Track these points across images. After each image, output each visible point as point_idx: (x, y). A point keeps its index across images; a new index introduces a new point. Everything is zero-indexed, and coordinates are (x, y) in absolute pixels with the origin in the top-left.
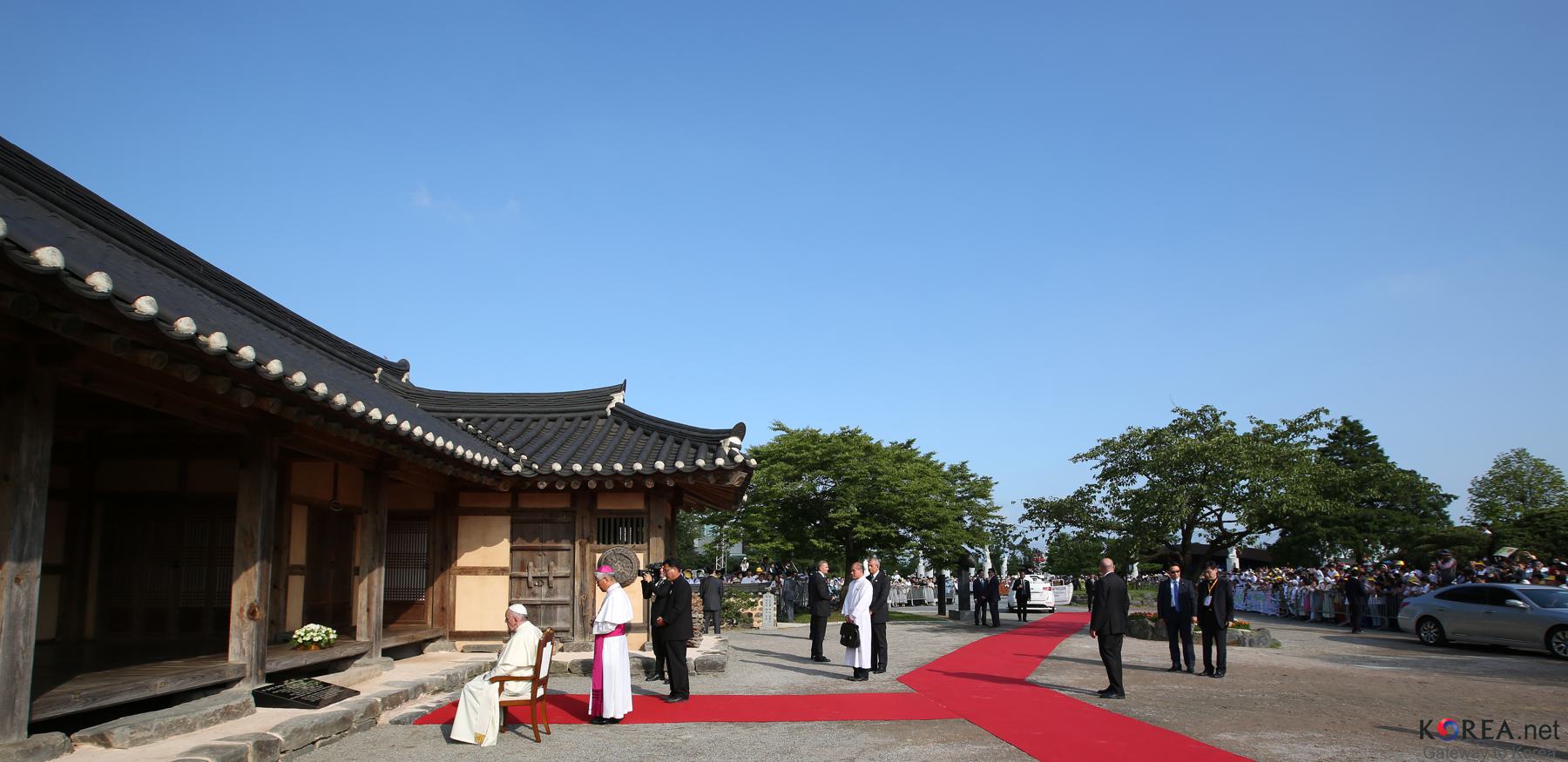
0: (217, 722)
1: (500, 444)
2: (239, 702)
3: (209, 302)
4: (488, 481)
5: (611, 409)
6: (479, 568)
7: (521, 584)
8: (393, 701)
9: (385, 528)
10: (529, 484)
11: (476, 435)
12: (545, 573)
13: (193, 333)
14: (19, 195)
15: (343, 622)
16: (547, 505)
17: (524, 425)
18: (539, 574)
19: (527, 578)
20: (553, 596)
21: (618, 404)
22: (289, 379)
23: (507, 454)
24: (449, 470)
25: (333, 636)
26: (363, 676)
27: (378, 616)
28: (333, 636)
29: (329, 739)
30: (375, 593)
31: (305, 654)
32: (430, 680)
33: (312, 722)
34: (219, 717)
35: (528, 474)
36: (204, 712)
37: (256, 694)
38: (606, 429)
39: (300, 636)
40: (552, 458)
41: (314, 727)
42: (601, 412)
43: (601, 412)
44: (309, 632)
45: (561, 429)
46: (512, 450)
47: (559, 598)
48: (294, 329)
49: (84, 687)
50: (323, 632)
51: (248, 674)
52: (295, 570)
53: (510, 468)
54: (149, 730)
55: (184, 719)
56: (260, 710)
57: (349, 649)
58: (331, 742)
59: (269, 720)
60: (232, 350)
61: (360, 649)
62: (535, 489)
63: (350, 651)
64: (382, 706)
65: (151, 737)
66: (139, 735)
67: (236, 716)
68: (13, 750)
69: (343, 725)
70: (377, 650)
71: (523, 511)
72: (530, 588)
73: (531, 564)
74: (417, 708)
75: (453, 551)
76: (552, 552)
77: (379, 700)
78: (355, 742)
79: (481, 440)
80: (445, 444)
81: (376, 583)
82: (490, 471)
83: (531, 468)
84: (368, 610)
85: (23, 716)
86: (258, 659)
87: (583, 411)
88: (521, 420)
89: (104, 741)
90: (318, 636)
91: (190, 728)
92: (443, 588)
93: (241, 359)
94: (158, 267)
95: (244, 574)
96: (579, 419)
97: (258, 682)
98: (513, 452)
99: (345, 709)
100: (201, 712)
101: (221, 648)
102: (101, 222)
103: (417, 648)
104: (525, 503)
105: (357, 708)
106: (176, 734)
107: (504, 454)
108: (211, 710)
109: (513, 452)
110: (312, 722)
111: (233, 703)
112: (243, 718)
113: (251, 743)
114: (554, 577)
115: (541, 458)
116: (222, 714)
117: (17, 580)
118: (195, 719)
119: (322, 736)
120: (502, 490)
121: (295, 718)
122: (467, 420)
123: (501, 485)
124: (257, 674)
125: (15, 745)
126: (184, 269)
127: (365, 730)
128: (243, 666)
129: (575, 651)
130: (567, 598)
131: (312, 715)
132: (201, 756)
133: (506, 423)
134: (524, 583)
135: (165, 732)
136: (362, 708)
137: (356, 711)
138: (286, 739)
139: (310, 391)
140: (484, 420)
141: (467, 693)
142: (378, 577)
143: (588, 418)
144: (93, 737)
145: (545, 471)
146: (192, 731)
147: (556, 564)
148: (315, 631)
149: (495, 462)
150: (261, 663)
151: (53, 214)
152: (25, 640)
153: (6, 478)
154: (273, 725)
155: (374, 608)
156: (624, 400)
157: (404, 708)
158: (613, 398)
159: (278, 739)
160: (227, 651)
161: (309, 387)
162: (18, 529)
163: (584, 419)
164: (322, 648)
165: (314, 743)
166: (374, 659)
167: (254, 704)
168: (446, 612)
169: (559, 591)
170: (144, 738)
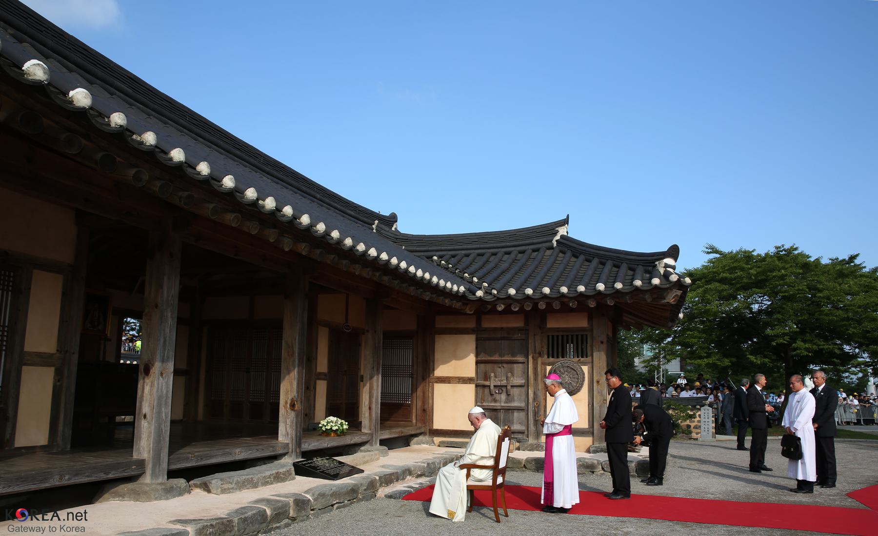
0: (272, 484)
1: (466, 275)
2: (284, 470)
3: (266, 180)
4: (457, 305)
5: (557, 241)
6: (451, 377)
7: (484, 391)
8: (388, 479)
9: (381, 345)
10: (489, 307)
11: (447, 269)
12: (504, 382)
13: (255, 199)
14: (166, 124)
15: (351, 414)
16: (505, 325)
17: (484, 258)
18: (499, 383)
19: (489, 386)
21: (562, 236)
22: (315, 228)
23: (472, 282)
24: (427, 296)
25: (345, 427)
26: (367, 458)
27: (376, 413)
28: (345, 427)
30: (375, 395)
31: (327, 439)
32: (414, 466)
33: (331, 489)
34: (272, 480)
35: (489, 298)
36: (264, 475)
37: (295, 465)
38: (553, 258)
39: (323, 425)
40: (508, 284)
41: (333, 492)
42: (548, 244)
43: (548, 244)
44: (329, 423)
45: (515, 260)
46: (475, 279)
47: (516, 404)
48: (318, 196)
49: (196, 450)
50: (339, 423)
51: (290, 450)
52: (320, 376)
53: (474, 294)
54: (231, 483)
55: (252, 478)
56: (298, 478)
57: (356, 438)
58: (344, 506)
59: (303, 485)
60: (278, 209)
61: (364, 438)
62: (494, 311)
63: (357, 439)
65: (233, 488)
66: (226, 486)
67: (283, 480)
68: (159, 487)
69: (353, 493)
70: (376, 439)
71: (486, 330)
72: (492, 395)
73: (492, 375)
74: (404, 487)
75: (432, 364)
76: (509, 366)
77: (377, 478)
78: (360, 508)
79: (451, 272)
80: (424, 275)
81: (375, 387)
82: (458, 296)
83: (491, 294)
84: (370, 408)
85: (165, 466)
86: (296, 440)
87: (533, 244)
88: (482, 255)
89: (206, 488)
90: (335, 426)
91: (255, 486)
92: (424, 393)
93: (284, 215)
94: (237, 161)
95: (287, 377)
96: (530, 251)
97: (297, 458)
98: (476, 281)
99: (353, 482)
100: (262, 475)
101: (273, 432)
102: (207, 135)
103: (404, 441)
104: (486, 324)
105: (362, 482)
106: (247, 489)
107: (469, 282)
108: (268, 473)
109: (476, 281)
110: (331, 489)
111: (281, 470)
112: (287, 482)
114: (511, 386)
115: (498, 285)
116: (275, 478)
117: (162, 374)
118: (258, 479)
119: (338, 501)
120: (468, 312)
121: (320, 485)
122: (440, 257)
123: (468, 308)
125: (161, 484)
126: (252, 160)
128: (287, 444)
129: (530, 450)
130: (523, 405)
132: (262, 505)
133: (470, 258)
134: (487, 390)
135: (241, 486)
136: (365, 483)
137: (361, 484)
138: (315, 500)
139: (328, 237)
140: (454, 256)
141: (442, 477)
142: (377, 383)
143: (537, 250)
144: (200, 484)
145: (502, 296)
146: (256, 487)
147: (513, 375)
148: (333, 422)
149: (462, 289)
150: (299, 444)
151: (183, 134)
152: (166, 416)
153: (157, 306)
155: (374, 406)
156: (567, 232)
158: (558, 231)
159: (309, 499)
160: (277, 434)
161: (327, 234)
162: (162, 340)
163: (534, 251)
164: (338, 436)
165: (332, 505)
166: (374, 447)
168: (427, 413)
169: (516, 398)
170: (229, 489)
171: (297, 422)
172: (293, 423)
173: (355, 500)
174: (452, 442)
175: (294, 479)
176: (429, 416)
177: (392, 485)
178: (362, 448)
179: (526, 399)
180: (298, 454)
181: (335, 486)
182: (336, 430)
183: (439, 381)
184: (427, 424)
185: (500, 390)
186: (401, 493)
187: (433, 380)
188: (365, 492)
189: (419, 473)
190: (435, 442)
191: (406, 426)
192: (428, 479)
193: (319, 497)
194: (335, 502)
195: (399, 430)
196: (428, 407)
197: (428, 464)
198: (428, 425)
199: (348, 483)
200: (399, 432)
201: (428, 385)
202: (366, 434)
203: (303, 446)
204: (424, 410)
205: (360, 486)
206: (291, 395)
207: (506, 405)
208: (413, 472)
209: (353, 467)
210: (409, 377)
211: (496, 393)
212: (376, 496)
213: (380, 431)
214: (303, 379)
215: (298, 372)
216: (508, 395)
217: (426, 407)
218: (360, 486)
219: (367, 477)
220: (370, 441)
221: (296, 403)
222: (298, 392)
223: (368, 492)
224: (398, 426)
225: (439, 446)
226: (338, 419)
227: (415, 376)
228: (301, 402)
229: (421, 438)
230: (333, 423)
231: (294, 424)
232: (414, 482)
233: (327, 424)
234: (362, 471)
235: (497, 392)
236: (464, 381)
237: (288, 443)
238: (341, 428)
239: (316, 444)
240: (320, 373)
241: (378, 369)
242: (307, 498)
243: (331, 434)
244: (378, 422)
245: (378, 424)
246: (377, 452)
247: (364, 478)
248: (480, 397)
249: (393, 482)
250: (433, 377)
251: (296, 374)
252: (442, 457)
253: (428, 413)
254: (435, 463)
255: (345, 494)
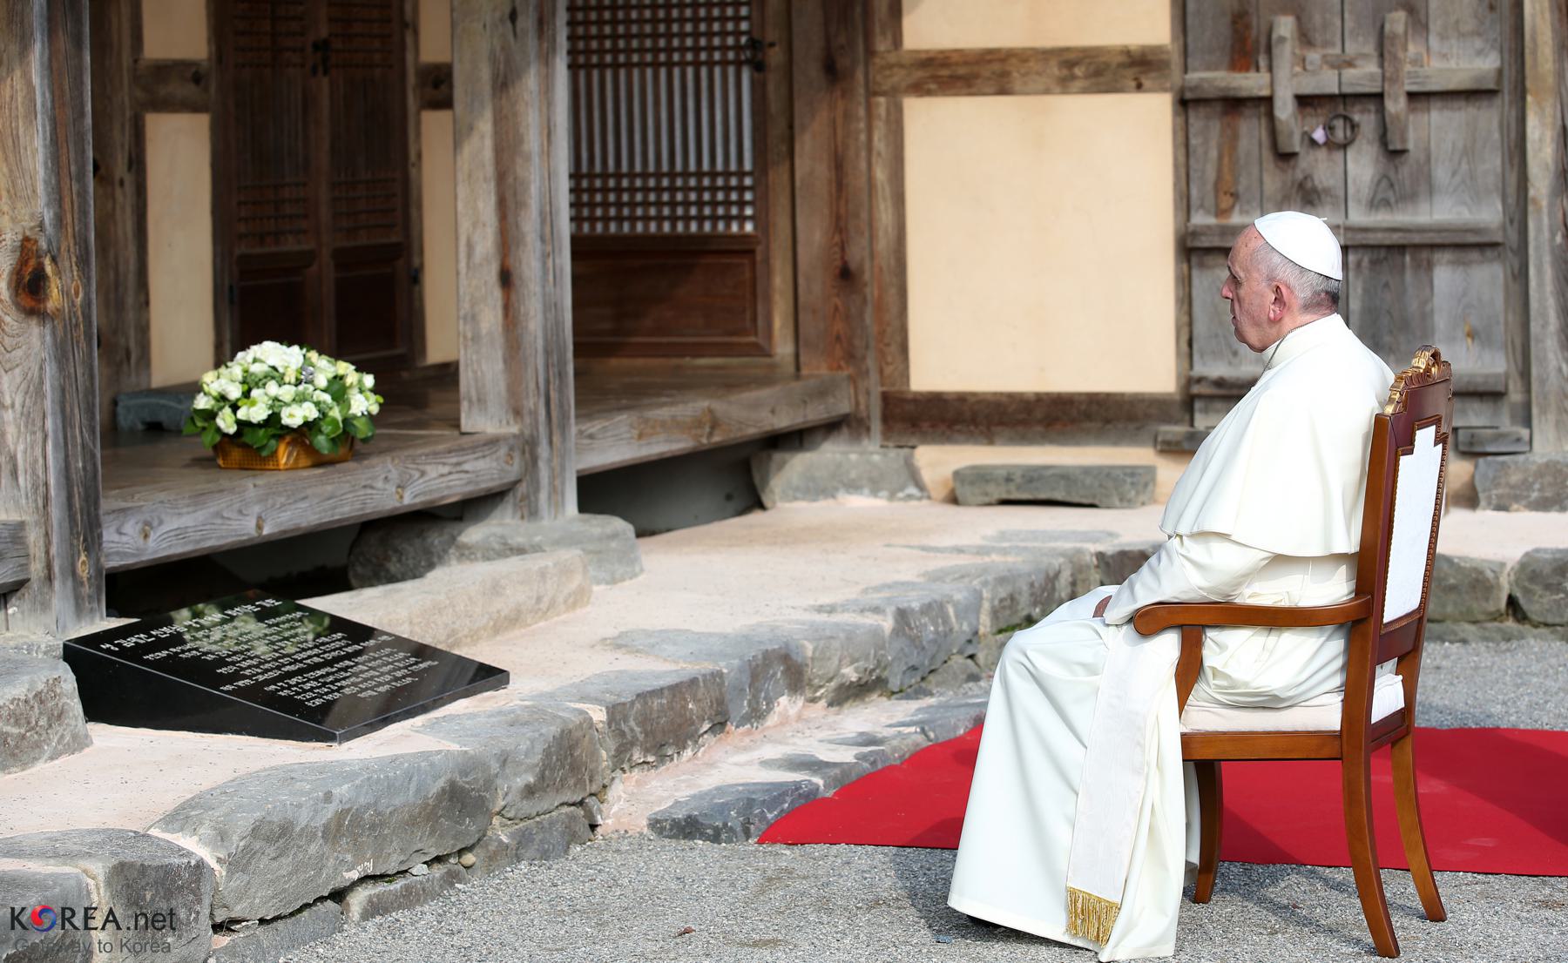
7: (1235, 137)
12: (1363, 75)
18: (1327, 82)
19: (1268, 101)
20: (1409, 197)
26: (517, 596)
27: (550, 306)
28: (363, 403)
29: (398, 885)
30: (534, 190)
31: (252, 486)
32: (816, 632)
33: (328, 797)
37: (77, 655)
39: (222, 398)
41: (340, 816)
44: (260, 382)
50: (322, 381)
51: (36, 569)
56: (107, 736)
57: (433, 471)
58: (410, 899)
61: (483, 471)
64: (612, 744)
72: (1285, 157)
73: (1285, 26)
74: (766, 764)
77: (599, 715)
81: (533, 141)
84: (506, 278)
90: (300, 399)
92: (839, 165)
99: (455, 747)
105: (508, 743)
110: (328, 797)
112: (42, 768)
113: (98, 869)
114: (1412, 96)
119: (369, 868)
124: (74, 573)
127: (545, 855)
129: (1543, 505)
130: (1489, 215)
131: (321, 769)
134: (1251, 131)
136: (529, 746)
137: (504, 760)
138: (235, 864)
154: (170, 802)
155: (530, 265)
157: (711, 765)
159: (200, 866)
164: (320, 462)
165: (339, 895)
166: (546, 522)
167: (76, 706)
169: (1441, 173)
171: (63, 390)
172: (39, 393)
173: (469, 858)
174: (1033, 475)
175: (79, 743)
176: (880, 308)
177: (688, 753)
178: (473, 534)
179: (1512, 179)
180: (86, 590)
181: (349, 777)
182: (309, 427)
183: (935, 78)
184: (871, 363)
185: (1339, 124)
186: (750, 803)
187: (899, 77)
188: (528, 807)
189: (850, 674)
190: (927, 476)
191: (730, 384)
192: (905, 709)
193: (257, 845)
194: (354, 875)
195: (693, 407)
196: (872, 256)
197: (902, 615)
198: (874, 376)
199: (425, 755)
200: (698, 423)
201: (862, 112)
202: (493, 442)
203: (109, 535)
204: (846, 276)
205: (495, 767)
206: (14, 220)
207: (1383, 218)
208: (814, 671)
209: (421, 651)
210: (738, 64)
211: (1313, 143)
212: (593, 827)
213: (577, 423)
214: (82, 114)
215: (52, 70)
216: (1392, 153)
217: (856, 254)
218: (495, 767)
219: (535, 714)
220: (522, 489)
221: (49, 269)
222: (57, 196)
223: (545, 806)
224: (683, 385)
225: (954, 500)
226: (313, 355)
227: (775, 56)
228: (83, 261)
229: (830, 454)
230: (281, 383)
231: (48, 404)
232: (825, 734)
233: (247, 394)
234: (488, 676)
235: (1319, 135)
236: (1098, 73)
237: (21, 525)
238: (336, 413)
239: (187, 521)
240: (164, 70)
241: (543, 24)
242: (189, 854)
243: (274, 454)
244: (562, 363)
245: (561, 375)
246: (570, 555)
247: (515, 722)
248: (1211, 174)
249: (695, 737)
250: (892, 58)
251: (36, 80)
252: (985, 570)
253: (871, 292)
254: (941, 606)
255: (412, 822)
